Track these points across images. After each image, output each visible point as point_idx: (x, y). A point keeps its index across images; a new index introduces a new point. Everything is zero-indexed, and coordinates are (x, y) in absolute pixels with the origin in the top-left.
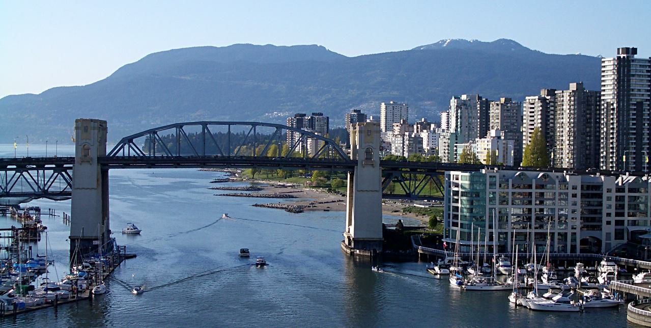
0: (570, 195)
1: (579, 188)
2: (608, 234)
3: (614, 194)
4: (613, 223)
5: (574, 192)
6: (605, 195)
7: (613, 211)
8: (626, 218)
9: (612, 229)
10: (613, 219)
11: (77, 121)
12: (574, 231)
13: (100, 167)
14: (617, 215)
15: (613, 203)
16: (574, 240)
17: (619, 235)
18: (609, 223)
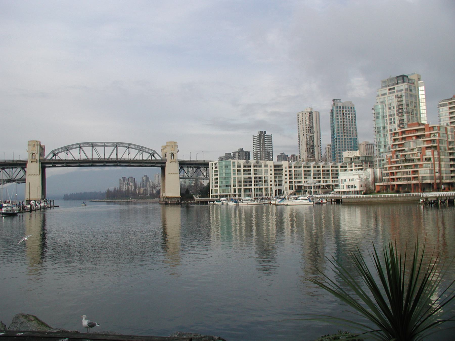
0: (269, 170)
1: (273, 167)
2: (286, 188)
3: (288, 169)
4: (288, 182)
5: (271, 168)
6: (284, 170)
7: (288, 177)
8: (293, 180)
9: (288, 185)
10: (288, 180)
11: (29, 142)
12: (271, 187)
13: (41, 164)
14: (290, 178)
15: (288, 173)
16: (271, 190)
17: (291, 188)
18: (286, 182)
